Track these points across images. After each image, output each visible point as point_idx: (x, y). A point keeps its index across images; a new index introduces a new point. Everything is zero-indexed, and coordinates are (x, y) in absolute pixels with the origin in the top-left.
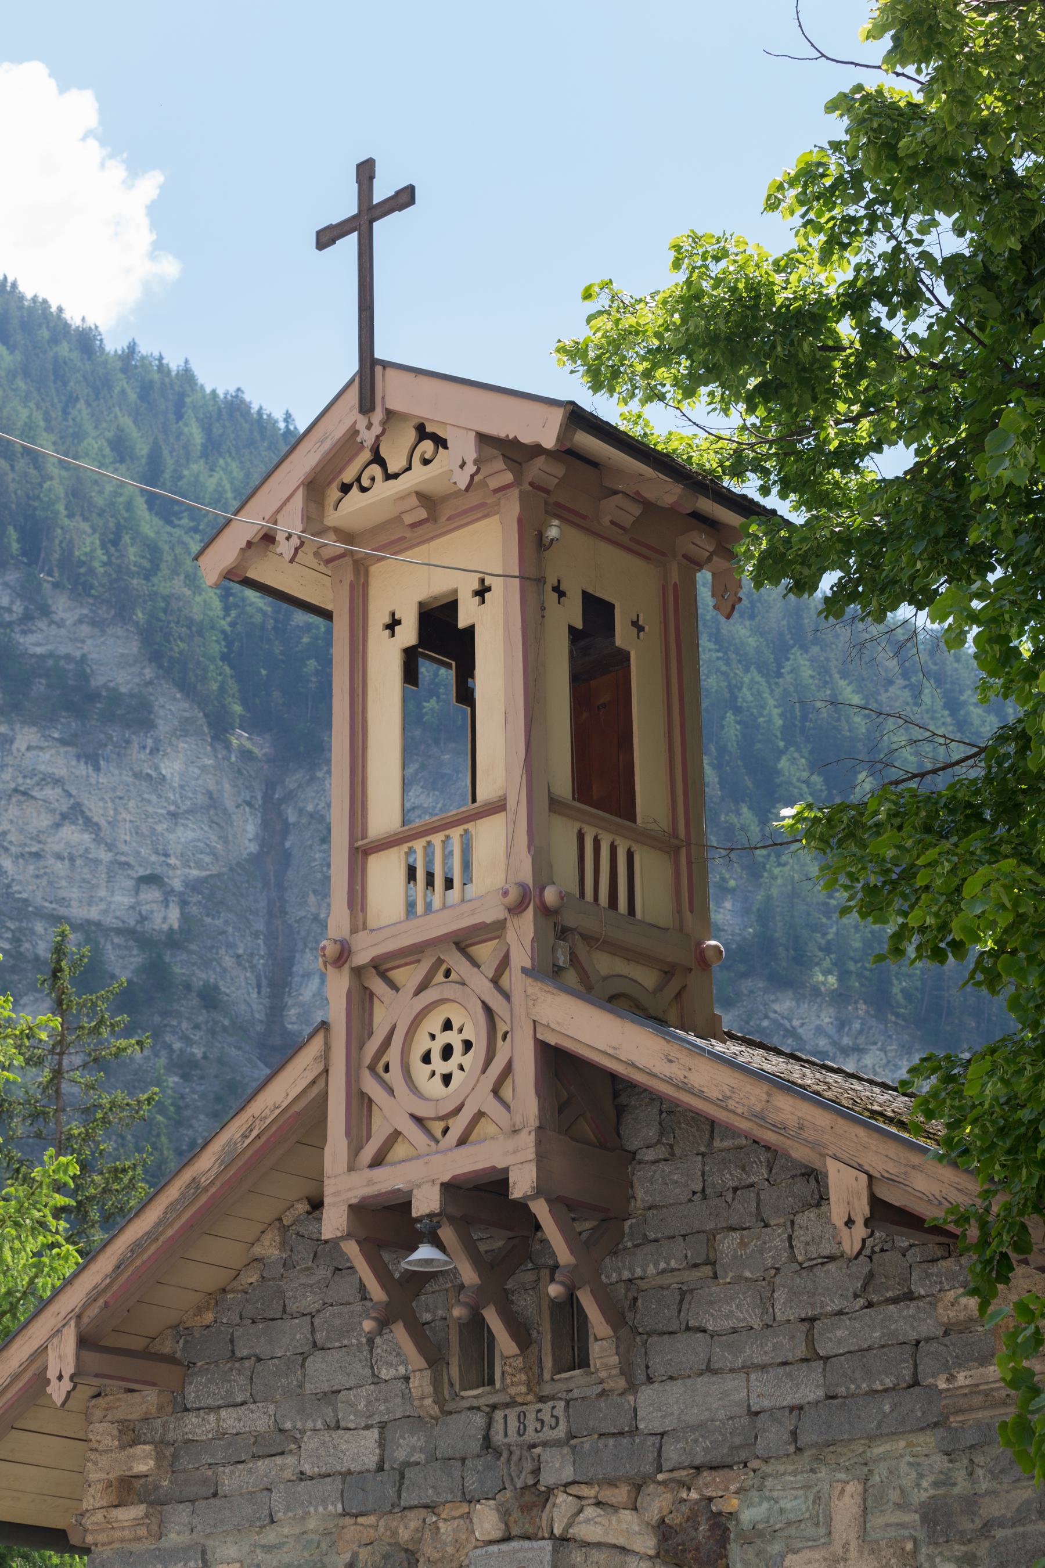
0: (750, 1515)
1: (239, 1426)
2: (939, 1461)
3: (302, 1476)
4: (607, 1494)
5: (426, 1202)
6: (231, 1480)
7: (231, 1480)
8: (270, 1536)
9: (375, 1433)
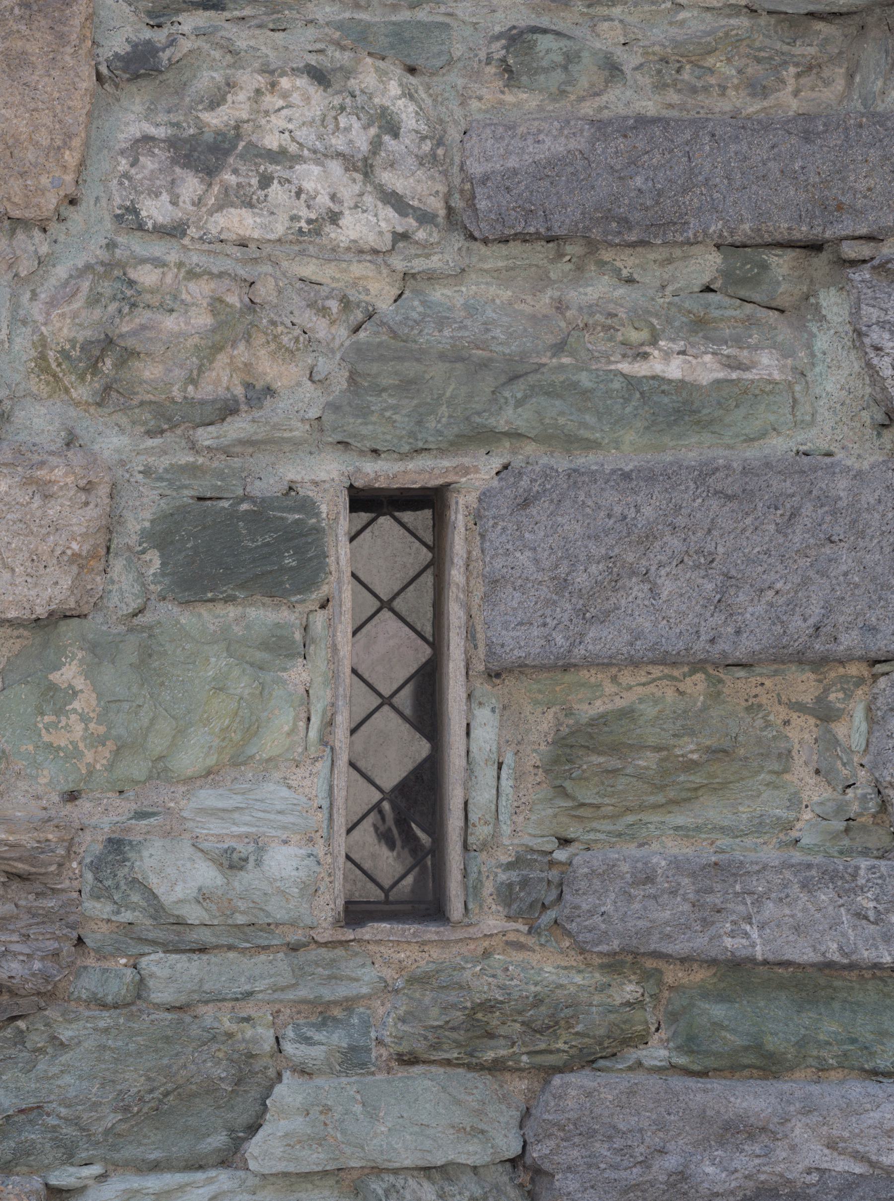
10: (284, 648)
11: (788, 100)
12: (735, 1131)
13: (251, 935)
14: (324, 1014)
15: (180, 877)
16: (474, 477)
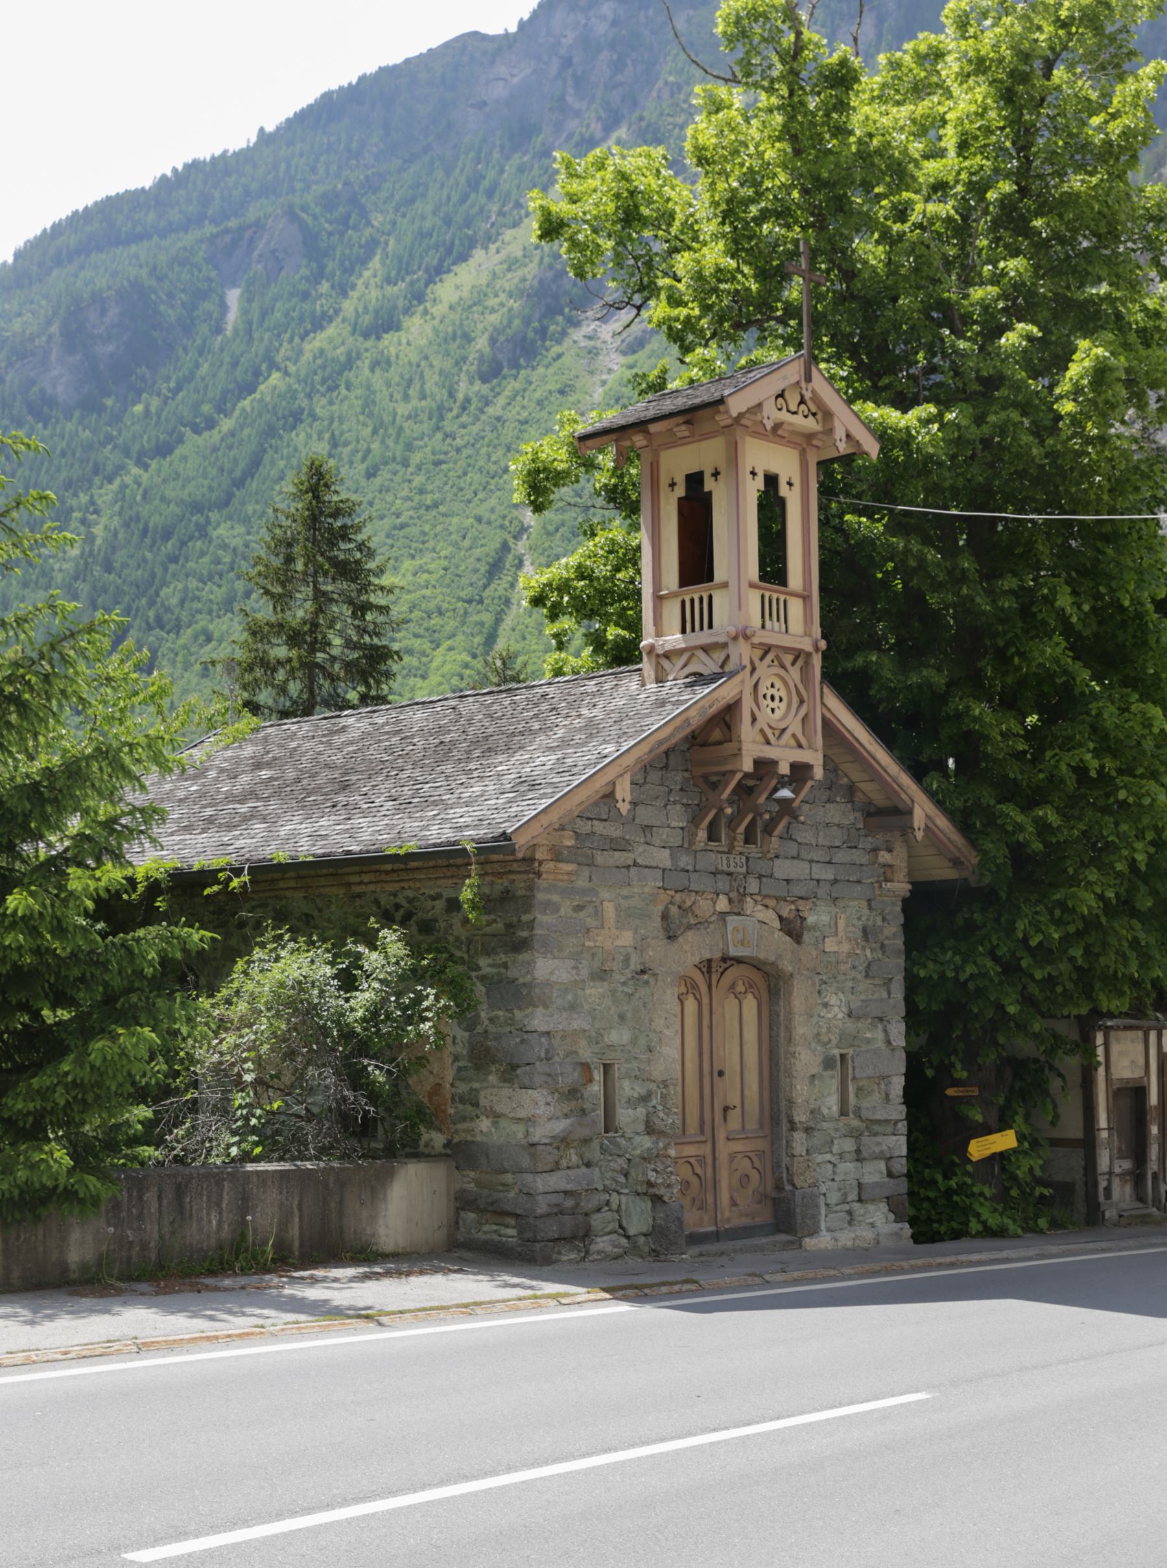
0: (811, 919)
1: (605, 832)
2: (866, 911)
3: (635, 864)
4: (766, 901)
5: (784, 769)
6: (600, 858)
7: (600, 858)
8: (625, 892)
9: (667, 851)
10: (832, 1077)
11: (876, 996)
12: (879, 1144)
13: (831, 1119)
14: (837, 1130)
15: (825, 1111)
16: (851, 1051)
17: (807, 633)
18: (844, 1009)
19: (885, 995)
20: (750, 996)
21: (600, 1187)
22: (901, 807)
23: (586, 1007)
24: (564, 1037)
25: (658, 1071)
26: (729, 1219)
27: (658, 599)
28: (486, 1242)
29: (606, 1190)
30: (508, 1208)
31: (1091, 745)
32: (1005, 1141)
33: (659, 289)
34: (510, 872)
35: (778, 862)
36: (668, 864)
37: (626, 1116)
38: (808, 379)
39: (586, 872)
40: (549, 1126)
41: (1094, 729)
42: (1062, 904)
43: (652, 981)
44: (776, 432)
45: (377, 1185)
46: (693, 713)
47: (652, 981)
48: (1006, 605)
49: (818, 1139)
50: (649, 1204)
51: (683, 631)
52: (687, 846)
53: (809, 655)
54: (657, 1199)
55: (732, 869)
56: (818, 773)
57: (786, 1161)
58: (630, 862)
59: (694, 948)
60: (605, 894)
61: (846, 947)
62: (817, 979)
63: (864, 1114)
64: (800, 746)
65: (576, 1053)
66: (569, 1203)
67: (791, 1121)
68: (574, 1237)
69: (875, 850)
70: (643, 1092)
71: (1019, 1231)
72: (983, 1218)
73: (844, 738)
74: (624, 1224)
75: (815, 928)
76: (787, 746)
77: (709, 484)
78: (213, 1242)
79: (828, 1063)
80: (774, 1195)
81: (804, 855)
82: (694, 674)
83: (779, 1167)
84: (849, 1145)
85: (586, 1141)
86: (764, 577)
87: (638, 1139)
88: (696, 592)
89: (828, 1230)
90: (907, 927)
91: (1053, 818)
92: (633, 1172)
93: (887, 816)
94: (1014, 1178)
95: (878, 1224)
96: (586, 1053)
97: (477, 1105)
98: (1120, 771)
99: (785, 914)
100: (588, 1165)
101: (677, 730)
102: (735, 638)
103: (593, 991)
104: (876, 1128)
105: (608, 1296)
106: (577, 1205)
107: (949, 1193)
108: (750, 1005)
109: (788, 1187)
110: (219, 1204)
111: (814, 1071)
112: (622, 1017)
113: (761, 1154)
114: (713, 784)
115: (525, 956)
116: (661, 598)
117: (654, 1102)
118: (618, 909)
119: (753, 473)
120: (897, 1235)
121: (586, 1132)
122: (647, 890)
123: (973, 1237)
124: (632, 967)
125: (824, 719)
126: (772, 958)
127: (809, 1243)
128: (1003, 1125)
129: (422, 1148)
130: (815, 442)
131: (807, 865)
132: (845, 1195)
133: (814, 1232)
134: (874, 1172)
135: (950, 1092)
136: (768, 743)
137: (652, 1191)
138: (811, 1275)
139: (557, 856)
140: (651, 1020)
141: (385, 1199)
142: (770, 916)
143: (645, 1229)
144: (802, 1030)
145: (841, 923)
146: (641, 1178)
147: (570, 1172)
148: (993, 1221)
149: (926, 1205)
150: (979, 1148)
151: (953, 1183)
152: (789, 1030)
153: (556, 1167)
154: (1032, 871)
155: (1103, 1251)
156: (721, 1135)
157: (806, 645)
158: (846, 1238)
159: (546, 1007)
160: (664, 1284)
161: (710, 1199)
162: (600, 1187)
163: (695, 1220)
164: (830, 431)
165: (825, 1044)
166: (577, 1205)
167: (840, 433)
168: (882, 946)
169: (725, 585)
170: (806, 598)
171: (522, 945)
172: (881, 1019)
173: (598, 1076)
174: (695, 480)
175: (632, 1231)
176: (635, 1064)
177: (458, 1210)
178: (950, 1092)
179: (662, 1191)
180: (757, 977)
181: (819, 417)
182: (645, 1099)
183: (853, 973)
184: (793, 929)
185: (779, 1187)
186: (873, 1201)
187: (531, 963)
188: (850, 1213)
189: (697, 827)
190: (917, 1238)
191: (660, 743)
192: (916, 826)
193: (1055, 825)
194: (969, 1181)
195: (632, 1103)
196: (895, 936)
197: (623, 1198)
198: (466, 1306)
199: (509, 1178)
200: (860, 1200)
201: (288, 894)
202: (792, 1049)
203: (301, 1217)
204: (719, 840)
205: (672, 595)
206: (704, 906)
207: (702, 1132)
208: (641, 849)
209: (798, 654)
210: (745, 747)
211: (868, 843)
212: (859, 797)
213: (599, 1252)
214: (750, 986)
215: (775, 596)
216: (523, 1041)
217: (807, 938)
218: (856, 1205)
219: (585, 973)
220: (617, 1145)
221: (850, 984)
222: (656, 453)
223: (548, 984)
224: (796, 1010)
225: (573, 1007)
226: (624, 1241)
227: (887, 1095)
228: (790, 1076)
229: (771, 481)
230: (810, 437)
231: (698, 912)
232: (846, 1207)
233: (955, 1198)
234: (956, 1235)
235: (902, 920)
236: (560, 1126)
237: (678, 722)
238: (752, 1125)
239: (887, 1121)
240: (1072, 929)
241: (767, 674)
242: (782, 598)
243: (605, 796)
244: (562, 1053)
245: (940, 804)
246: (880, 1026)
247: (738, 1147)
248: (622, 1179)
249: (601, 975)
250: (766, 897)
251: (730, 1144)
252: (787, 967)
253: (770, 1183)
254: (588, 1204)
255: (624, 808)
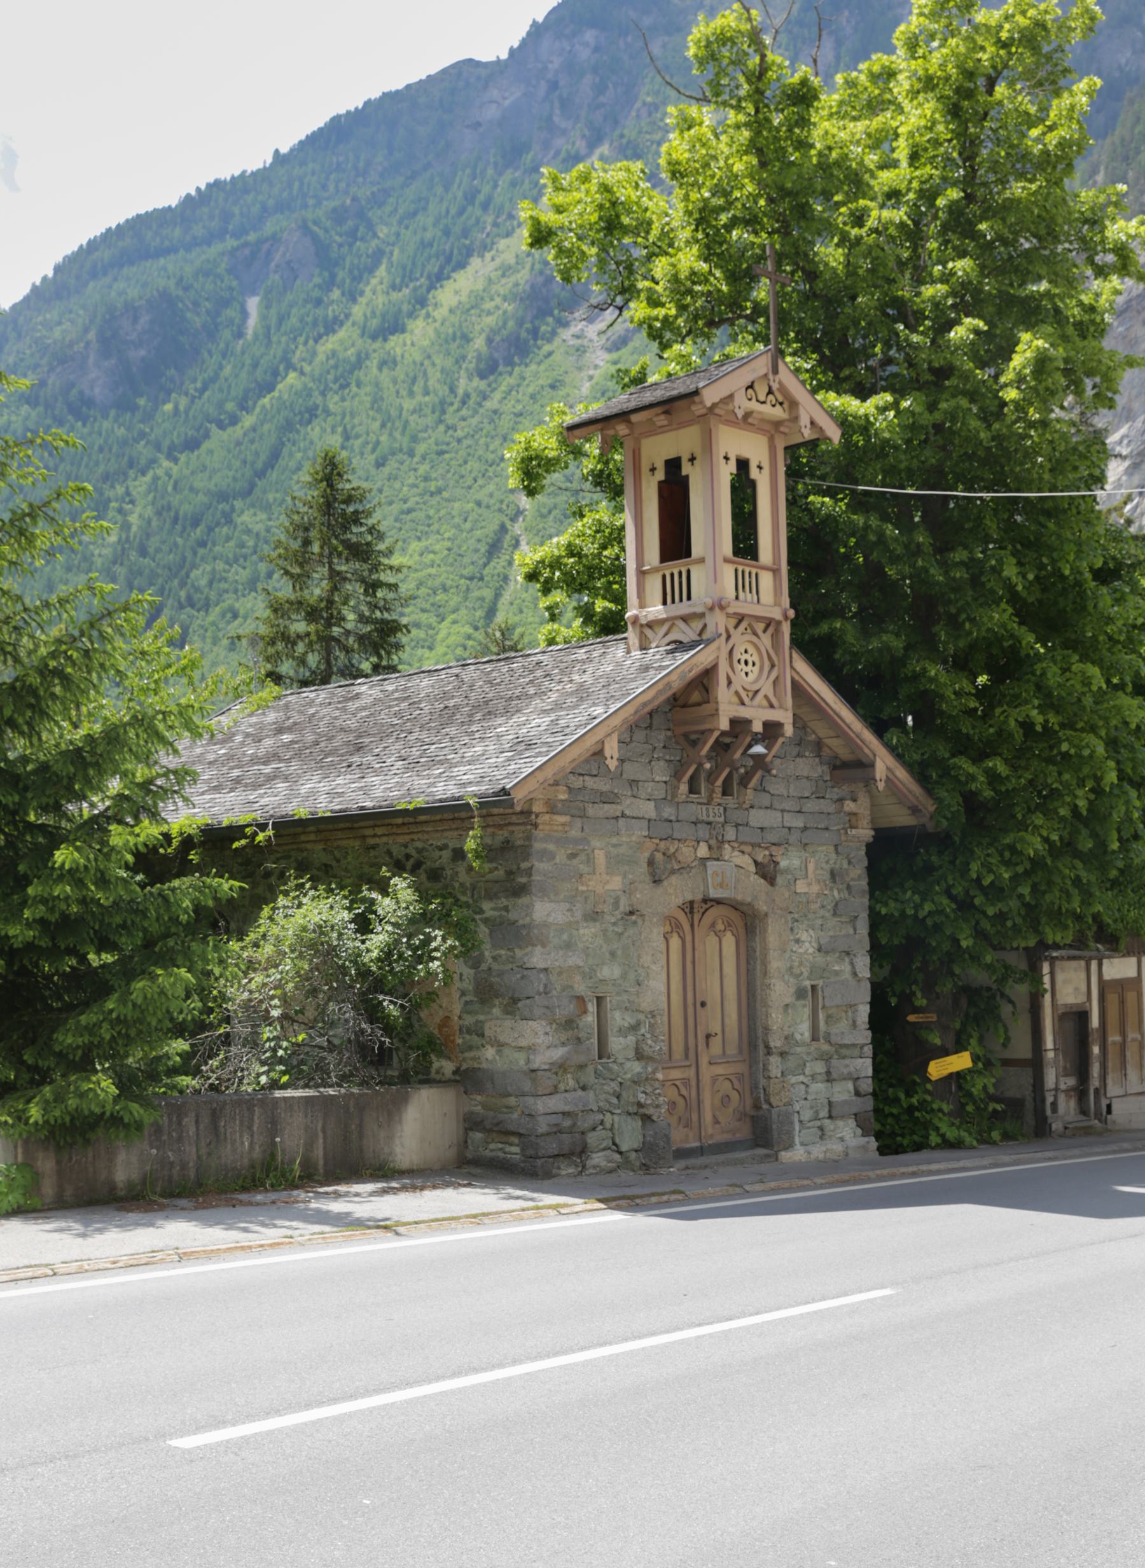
0: (783, 864)
1: (595, 787)
2: (834, 856)
3: (623, 815)
4: (743, 848)
5: (757, 727)
6: (591, 811)
7: (591, 811)
8: (614, 840)
9: (652, 804)
12: (847, 1066)
13: (804, 1044)
14: (809, 1054)
15: (798, 1037)
16: (820, 983)
17: (777, 603)
18: (815, 945)
19: (851, 931)
20: (729, 934)
21: (595, 1108)
22: (864, 760)
23: (580, 945)
24: (560, 973)
25: (646, 1003)
26: (712, 1136)
27: (641, 574)
28: (492, 1160)
29: (600, 1111)
30: (511, 1128)
31: (1036, 702)
32: (961, 1061)
33: (639, 291)
34: (510, 824)
35: (753, 812)
36: (653, 815)
37: (618, 1044)
38: (775, 371)
39: (578, 823)
40: (548, 1054)
41: (1039, 687)
42: (1012, 848)
43: (640, 922)
44: (747, 421)
45: (393, 1109)
46: (674, 677)
47: (640, 922)
48: (958, 575)
49: (792, 1062)
50: (640, 1123)
51: (665, 603)
52: (670, 798)
53: (779, 623)
54: (647, 1119)
55: (711, 819)
56: (789, 730)
57: (763, 1082)
58: (619, 814)
59: (678, 891)
60: (596, 843)
61: (815, 888)
62: (789, 917)
63: (833, 1039)
64: (772, 706)
65: (572, 987)
66: (567, 1123)
67: (767, 1047)
68: (572, 1154)
69: (841, 800)
70: (633, 1022)
71: (975, 1143)
72: (942, 1131)
73: (811, 697)
74: (617, 1141)
75: (787, 871)
76: (760, 706)
77: (686, 469)
78: (246, 1161)
79: (800, 994)
80: (753, 1113)
81: (776, 805)
82: (675, 642)
83: (757, 1087)
84: (820, 1067)
85: (582, 1067)
86: (737, 552)
87: (628, 1065)
88: (675, 567)
89: (802, 1144)
90: (871, 869)
91: (1002, 768)
92: (624, 1094)
93: (851, 769)
94: (969, 1095)
95: (847, 1138)
96: (581, 987)
97: (482, 1035)
98: (1063, 726)
99: (760, 859)
100: (584, 1088)
101: (659, 692)
102: (711, 609)
103: (586, 931)
104: (844, 1051)
105: (603, 1206)
106: (574, 1124)
107: (911, 1109)
108: (729, 941)
109: (765, 1106)
110: (250, 1128)
111: (788, 1000)
112: (613, 954)
113: (740, 1077)
114: (693, 741)
115: (524, 900)
116: (644, 573)
117: (643, 1031)
118: (608, 856)
119: (726, 458)
120: (864, 1148)
121: (582, 1059)
122: (634, 838)
123: (933, 1148)
124: (622, 908)
125: (793, 681)
126: (749, 899)
127: (785, 1156)
128: (959, 1048)
129: (433, 1075)
130: (782, 429)
131: (779, 814)
132: (817, 1112)
133: (789, 1146)
134: (843, 1092)
135: (911, 1018)
136: (743, 704)
137: (642, 1111)
138: (787, 1185)
139: (552, 809)
140: (639, 957)
141: (400, 1122)
142: (746, 862)
143: (636, 1146)
144: (776, 964)
145: (811, 867)
146: (632, 1099)
147: (567, 1095)
148: (951, 1134)
149: (890, 1120)
150: (937, 1069)
151: (914, 1101)
152: (765, 964)
153: (555, 1091)
154: (982, 817)
155: (1050, 1159)
156: (704, 1060)
157: (777, 615)
158: (818, 1152)
159: (544, 946)
160: (653, 1195)
161: (695, 1117)
162: (595, 1108)
163: (681, 1137)
164: (795, 419)
165: (797, 976)
166: (574, 1124)
167: (804, 420)
168: (849, 887)
169: (702, 560)
170: (775, 571)
171: (520, 891)
172: (848, 953)
173: (592, 1007)
174: (673, 465)
175: (624, 1148)
176: (625, 997)
177: (467, 1130)
178: (911, 1018)
179: (650, 1111)
180: (734, 916)
181: (786, 405)
182: (634, 1028)
183: (822, 912)
184: (767, 872)
185: (757, 1107)
186: (842, 1117)
187: (530, 907)
188: (821, 1128)
189: (679, 781)
190: (883, 1151)
191: (645, 705)
192: (878, 777)
193: (1004, 775)
194: (929, 1098)
195: (622, 1032)
196: (859, 877)
197: (616, 1118)
198: (475, 1216)
199: (512, 1101)
200: (830, 1117)
201: (309, 846)
202: (767, 981)
203: (325, 1138)
204: (699, 793)
205: (654, 570)
206: (686, 853)
207: (687, 1057)
208: (628, 802)
209: (769, 623)
210: (722, 707)
211: (835, 793)
212: (826, 752)
213: (594, 1167)
214: (729, 925)
215: (747, 570)
216: (523, 977)
217: (779, 880)
218: (827, 1122)
219: (579, 915)
220: (610, 1070)
221: (819, 922)
222: (638, 441)
223: (545, 925)
224: (771, 946)
225: (568, 946)
226: (617, 1157)
227: (854, 1022)
228: (766, 1005)
229: (743, 465)
230: (777, 424)
231: (680, 858)
232: (818, 1123)
233: (917, 1114)
234: (918, 1147)
235: (866, 863)
236: (558, 1054)
237: (660, 686)
238: (732, 1050)
239: (854, 1045)
240: (1020, 869)
241: (741, 641)
242: (754, 571)
243: (595, 754)
244: (559, 988)
245: (899, 757)
246: (847, 959)
247: (719, 1070)
248: (615, 1101)
249: (593, 916)
250: (742, 843)
251: (713, 1067)
252: (763, 907)
253: (749, 1102)
254: (584, 1123)
255: (612, 764)
